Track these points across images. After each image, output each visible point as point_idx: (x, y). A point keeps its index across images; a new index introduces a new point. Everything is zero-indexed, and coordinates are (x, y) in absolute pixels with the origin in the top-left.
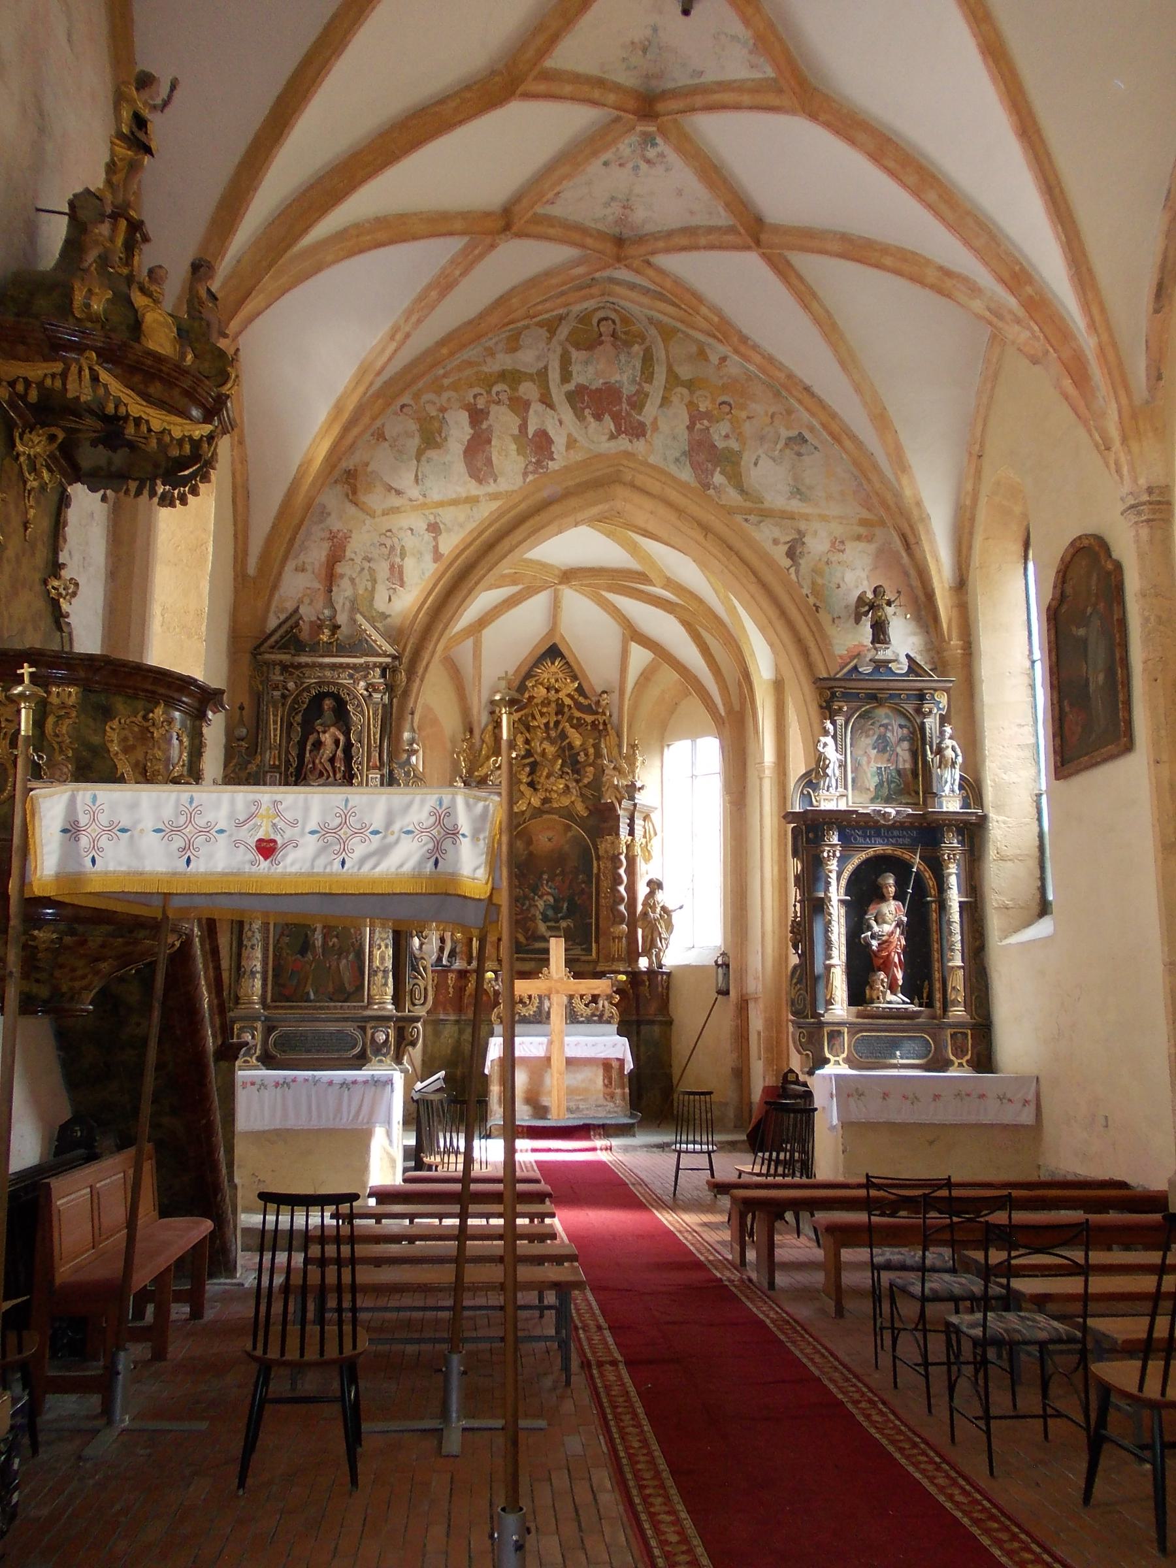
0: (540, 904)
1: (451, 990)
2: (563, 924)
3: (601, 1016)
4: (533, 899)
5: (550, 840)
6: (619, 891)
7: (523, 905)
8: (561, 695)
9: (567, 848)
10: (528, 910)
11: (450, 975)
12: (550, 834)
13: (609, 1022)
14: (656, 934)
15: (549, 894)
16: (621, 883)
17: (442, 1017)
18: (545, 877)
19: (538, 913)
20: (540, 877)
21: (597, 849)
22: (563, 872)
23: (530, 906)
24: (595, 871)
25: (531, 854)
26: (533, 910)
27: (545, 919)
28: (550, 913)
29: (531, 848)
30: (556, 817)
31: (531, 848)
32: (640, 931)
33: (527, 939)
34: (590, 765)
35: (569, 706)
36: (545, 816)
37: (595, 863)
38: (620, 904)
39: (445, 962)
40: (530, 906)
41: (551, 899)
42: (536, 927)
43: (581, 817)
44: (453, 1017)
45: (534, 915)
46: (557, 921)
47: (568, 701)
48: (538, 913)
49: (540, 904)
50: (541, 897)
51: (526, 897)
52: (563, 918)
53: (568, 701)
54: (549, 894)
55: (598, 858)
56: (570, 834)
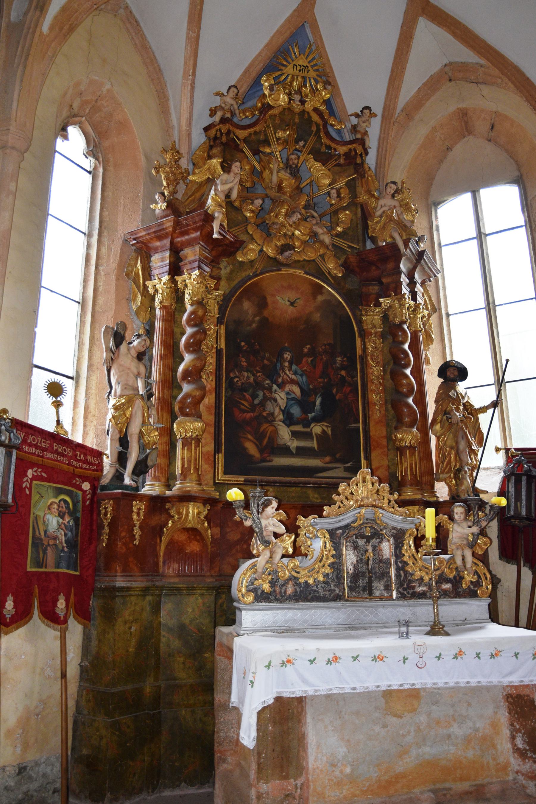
0: (281, 397)
1: (137, 532)
2: (317, 429)
3: (457, 581)
4: (270, 389)
5: (292, 304)
6: (406, 376)
7: (254, 396)
8: (308, 107)
9: (317, 317)
10: (262, 404)
11: (136, 505)
12: (292, 295)
13: (472, 594)
14: (462, 445)
15: (292, 382)
16: (406, 366)
17: (120, 582)
18: (287, 356)
19: (277, 411)
20: (280, 357)
21: (360, 322)
22: (313, 353)
23: (265, 399)
24: (359, 352)
25: (265, 323)
26: (269, 406)
27: (289, 420)
28: (296, 411)
29: (266, 313)
30: (300, 272)
31: (266, 313)
32: (433, 439)
33: (261, 451)
34: (345, 209)
35: (318, 125)
36: (284, 271)
37: (358, 340)
38: (408, 396)
39: (127, 481)
40: (265, 399)
41: (297, 390)
42: (276, 431)
43: (335, 278)
44: (139, 583)
45: (272, 414)
46: (307, 423)
47: (315, 117)
48: (277, 411)
49: (281, 397)
50: (281, 386)
51: (258, 385)
52: (317, 420)
53: (315, 117)
54: (292, 382)
55: (363, 334)
56: (320, 298)
